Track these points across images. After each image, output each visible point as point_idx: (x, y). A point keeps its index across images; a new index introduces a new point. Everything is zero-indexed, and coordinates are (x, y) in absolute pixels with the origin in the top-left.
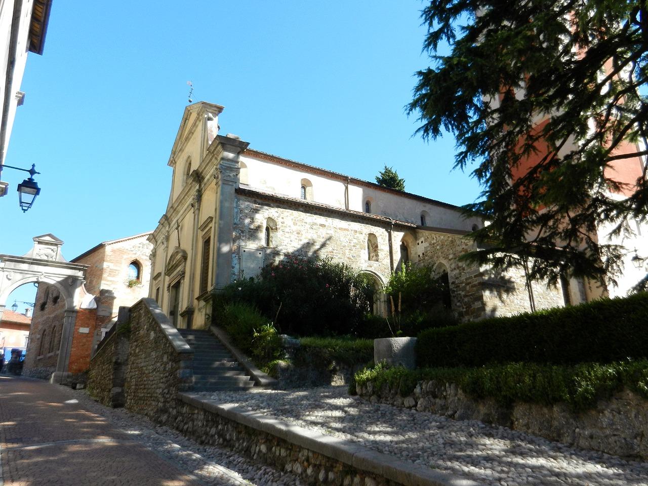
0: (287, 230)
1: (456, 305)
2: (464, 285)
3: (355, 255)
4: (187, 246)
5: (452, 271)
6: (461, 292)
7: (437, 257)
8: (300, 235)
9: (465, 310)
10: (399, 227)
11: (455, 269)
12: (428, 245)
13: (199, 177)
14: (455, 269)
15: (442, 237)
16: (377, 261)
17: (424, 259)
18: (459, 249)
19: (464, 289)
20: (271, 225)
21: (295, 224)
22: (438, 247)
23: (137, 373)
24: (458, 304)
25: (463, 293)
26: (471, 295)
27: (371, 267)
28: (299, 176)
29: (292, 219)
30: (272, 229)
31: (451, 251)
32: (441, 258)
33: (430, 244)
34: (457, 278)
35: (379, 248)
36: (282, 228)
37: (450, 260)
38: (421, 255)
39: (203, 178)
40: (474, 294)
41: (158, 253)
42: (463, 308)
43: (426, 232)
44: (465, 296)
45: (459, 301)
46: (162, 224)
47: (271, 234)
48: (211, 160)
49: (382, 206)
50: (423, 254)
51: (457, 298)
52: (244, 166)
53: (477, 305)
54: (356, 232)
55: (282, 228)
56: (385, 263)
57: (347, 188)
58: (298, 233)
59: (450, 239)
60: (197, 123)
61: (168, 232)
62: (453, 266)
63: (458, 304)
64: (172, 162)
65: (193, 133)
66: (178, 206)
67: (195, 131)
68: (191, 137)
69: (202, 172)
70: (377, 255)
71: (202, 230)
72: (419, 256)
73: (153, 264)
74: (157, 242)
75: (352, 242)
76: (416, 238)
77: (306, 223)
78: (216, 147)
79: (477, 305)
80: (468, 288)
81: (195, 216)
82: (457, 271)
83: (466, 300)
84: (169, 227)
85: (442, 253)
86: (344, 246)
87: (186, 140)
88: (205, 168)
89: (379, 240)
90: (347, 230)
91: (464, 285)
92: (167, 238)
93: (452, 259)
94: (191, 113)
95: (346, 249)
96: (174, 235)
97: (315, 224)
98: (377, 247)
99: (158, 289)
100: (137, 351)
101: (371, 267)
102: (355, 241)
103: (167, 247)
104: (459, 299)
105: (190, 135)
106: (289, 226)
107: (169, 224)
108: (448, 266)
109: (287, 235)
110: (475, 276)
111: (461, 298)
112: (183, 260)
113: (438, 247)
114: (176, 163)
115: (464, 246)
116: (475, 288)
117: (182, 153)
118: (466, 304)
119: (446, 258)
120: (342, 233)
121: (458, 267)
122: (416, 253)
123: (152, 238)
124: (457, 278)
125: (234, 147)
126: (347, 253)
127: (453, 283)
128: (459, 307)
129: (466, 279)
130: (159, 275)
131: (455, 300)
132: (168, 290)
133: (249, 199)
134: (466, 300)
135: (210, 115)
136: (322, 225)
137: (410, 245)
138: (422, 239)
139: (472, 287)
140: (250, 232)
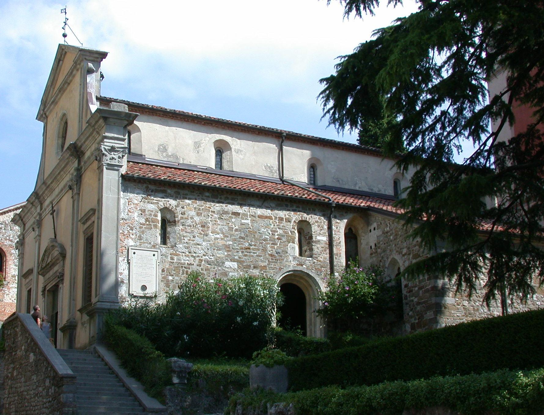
0: (189, 222)
1: (408, 314)
2: (417, 289)
3: (280, 251)
4: (65, 238)
7: (390, 251)
8: (206, 229)
9: (417, 321)
10: (342, 210)
12: (381, 233)
13: (77, 151)
16: (311, 257)
17: (376, 252)
20: (168, 217)
21: (199, 214)
23: (16, 398)
25: (416, 300)
26: (424, 302)
27: (302, 265)
28: (208, 139)
29: (195, 208)
30: (169, 222)
31: (405, 244)
32: (395, 252)
33: (383, 233)
35: (314, 239)
36: (182, 221)
37: (404, 255)
38: (373, 247)
39: (83, 153)
40: (427, 301)
41: (27, 240)
42: (415, 319)
44: (418, 303)
45: (411, 310)
46: (32, 203)
47: (169, 229)
48: (92, 133)
49: (333, 171)
50: (375, 245)
52: (138, 130)
54: (281, 219)
55: (182, 221)
56: (321, 260)
57: (281, 150)
58: (203, 226)
60: (74, 72)
61: (40, 215)
63: (410, 313)
64: (42, 116)
65: (69, 84)
66: (52, 183)
67: (71, 81)
68: (66, 89)
69: (81, 147)
70: (311, 250)
71: (84, 223)
72: (371, 247)
73: (21, 256)
74: (25, 225)
75: (276, 234)
76: (368, 224)
77: (214, 212)
78: (97, 122)
81: (74, 202)
84: (41, 209)
85: (395, 245)
86: (265, 240)
87: (60, 91)
88: (84, 142)
89: (315, 228)
90: (270, 218)
92: (39, 223)
93: (405, 254)
94: (66, 53)
95: (267, 244)
96: (48, 221)
97: (226, 213)
98: (311, 237)
99: (29, 291)
100: (15, 374)
101: (302, 265)
102: (280, 232)
103: (40, 236)
105: (66, 86)
106: (192, 218)
107: (41, 204)
109: (189, 229)
111: (414, 306)
112: (61, 258)
113: (391, 237)
114: (47, 117)
117: (55, 106)
119: (400, 253)
120: (262, 222)
122: (367, 244)
123: (19, 220)
125: (119, 121)
126: (269, 249)
128: (411, 317)
130: (30, 272)
132: (43, 294)
133: (140, 185)
134: (418, 308)
135: (90, 65)
136: (236, 214)
137: (360, 232)
138: (375, 225)
140: (140, 227)
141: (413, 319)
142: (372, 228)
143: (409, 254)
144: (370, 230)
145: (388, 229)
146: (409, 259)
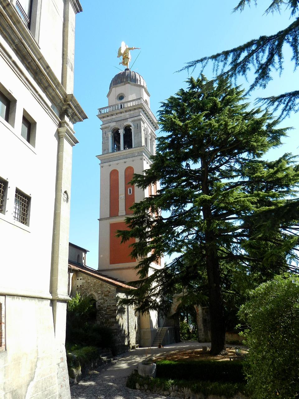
1: (99, 318)
2: (106, 308)
5: (99, 299)
6: (103, 312)
9: (104, 321)
11: (101, 299)
14: (101, 299)
15: (95, 281)
18: (106, 290)
19: (105, 310)
22: (92, 285)
24: (101, 317)
26: (109, 314)
32: (93, 291)
34: (102, 304)
38: (79, 286)
42: (104, 320)
43: (84, 274)
44: (106, 314)
45: (101, 316)
50: (81, 286)
51: (101, 314)
53: (112, 320)
59: (100, 283)
62: (100, 297)
63: (101, 317)
72: (78, 286)
76: (77, 276)
79: (112, 320)
80: (108, 310)
82: (103, 301)
83: (106, 316)
85: (94, 289)
91: (106, 308)
93: (100, 293)
104: (102, 315)
108: (96, 297)
110: (113, 306)
111: (103, 314)
113: (92, 285)
115: (108, 289)
116: (112, 312)
118: (105, 318)
119: (96, 292)
121: (103, 299)
122: (76, 284)
124: (102, 304)
127: (99, 306)
128: (101, 319)
129: (107, 306)
131: (100, 315)
138: (81, 278)
139: (111, 310)
141: (103, 320)
142: (79, 278)
143: (103, 294)
144: (78, 279)
145: (90, 281)
146: (102, 296)
